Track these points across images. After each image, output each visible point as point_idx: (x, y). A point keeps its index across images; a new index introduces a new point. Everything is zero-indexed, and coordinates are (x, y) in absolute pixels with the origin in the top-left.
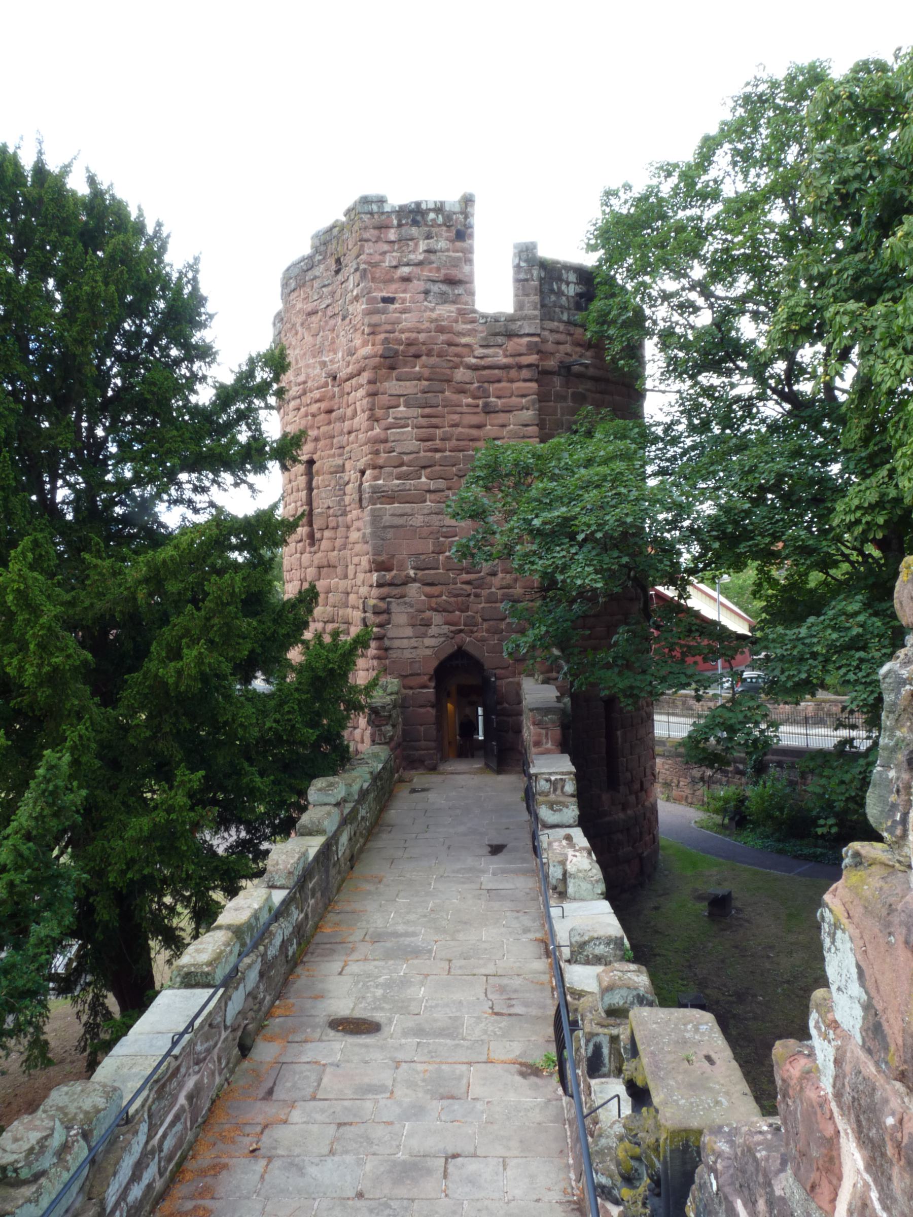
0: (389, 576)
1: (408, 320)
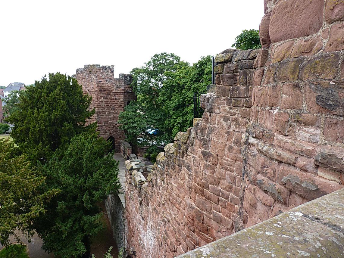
0: (100, 125)
1: (104, 85)
